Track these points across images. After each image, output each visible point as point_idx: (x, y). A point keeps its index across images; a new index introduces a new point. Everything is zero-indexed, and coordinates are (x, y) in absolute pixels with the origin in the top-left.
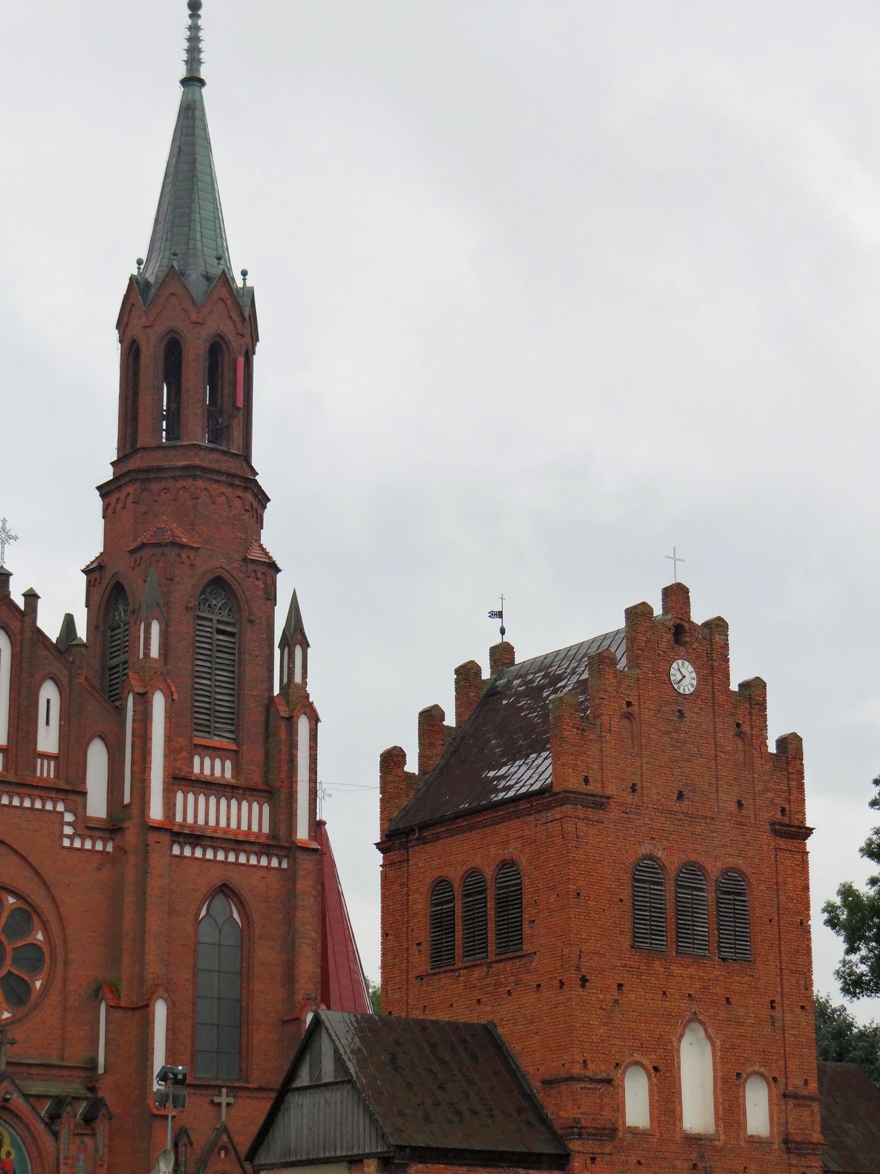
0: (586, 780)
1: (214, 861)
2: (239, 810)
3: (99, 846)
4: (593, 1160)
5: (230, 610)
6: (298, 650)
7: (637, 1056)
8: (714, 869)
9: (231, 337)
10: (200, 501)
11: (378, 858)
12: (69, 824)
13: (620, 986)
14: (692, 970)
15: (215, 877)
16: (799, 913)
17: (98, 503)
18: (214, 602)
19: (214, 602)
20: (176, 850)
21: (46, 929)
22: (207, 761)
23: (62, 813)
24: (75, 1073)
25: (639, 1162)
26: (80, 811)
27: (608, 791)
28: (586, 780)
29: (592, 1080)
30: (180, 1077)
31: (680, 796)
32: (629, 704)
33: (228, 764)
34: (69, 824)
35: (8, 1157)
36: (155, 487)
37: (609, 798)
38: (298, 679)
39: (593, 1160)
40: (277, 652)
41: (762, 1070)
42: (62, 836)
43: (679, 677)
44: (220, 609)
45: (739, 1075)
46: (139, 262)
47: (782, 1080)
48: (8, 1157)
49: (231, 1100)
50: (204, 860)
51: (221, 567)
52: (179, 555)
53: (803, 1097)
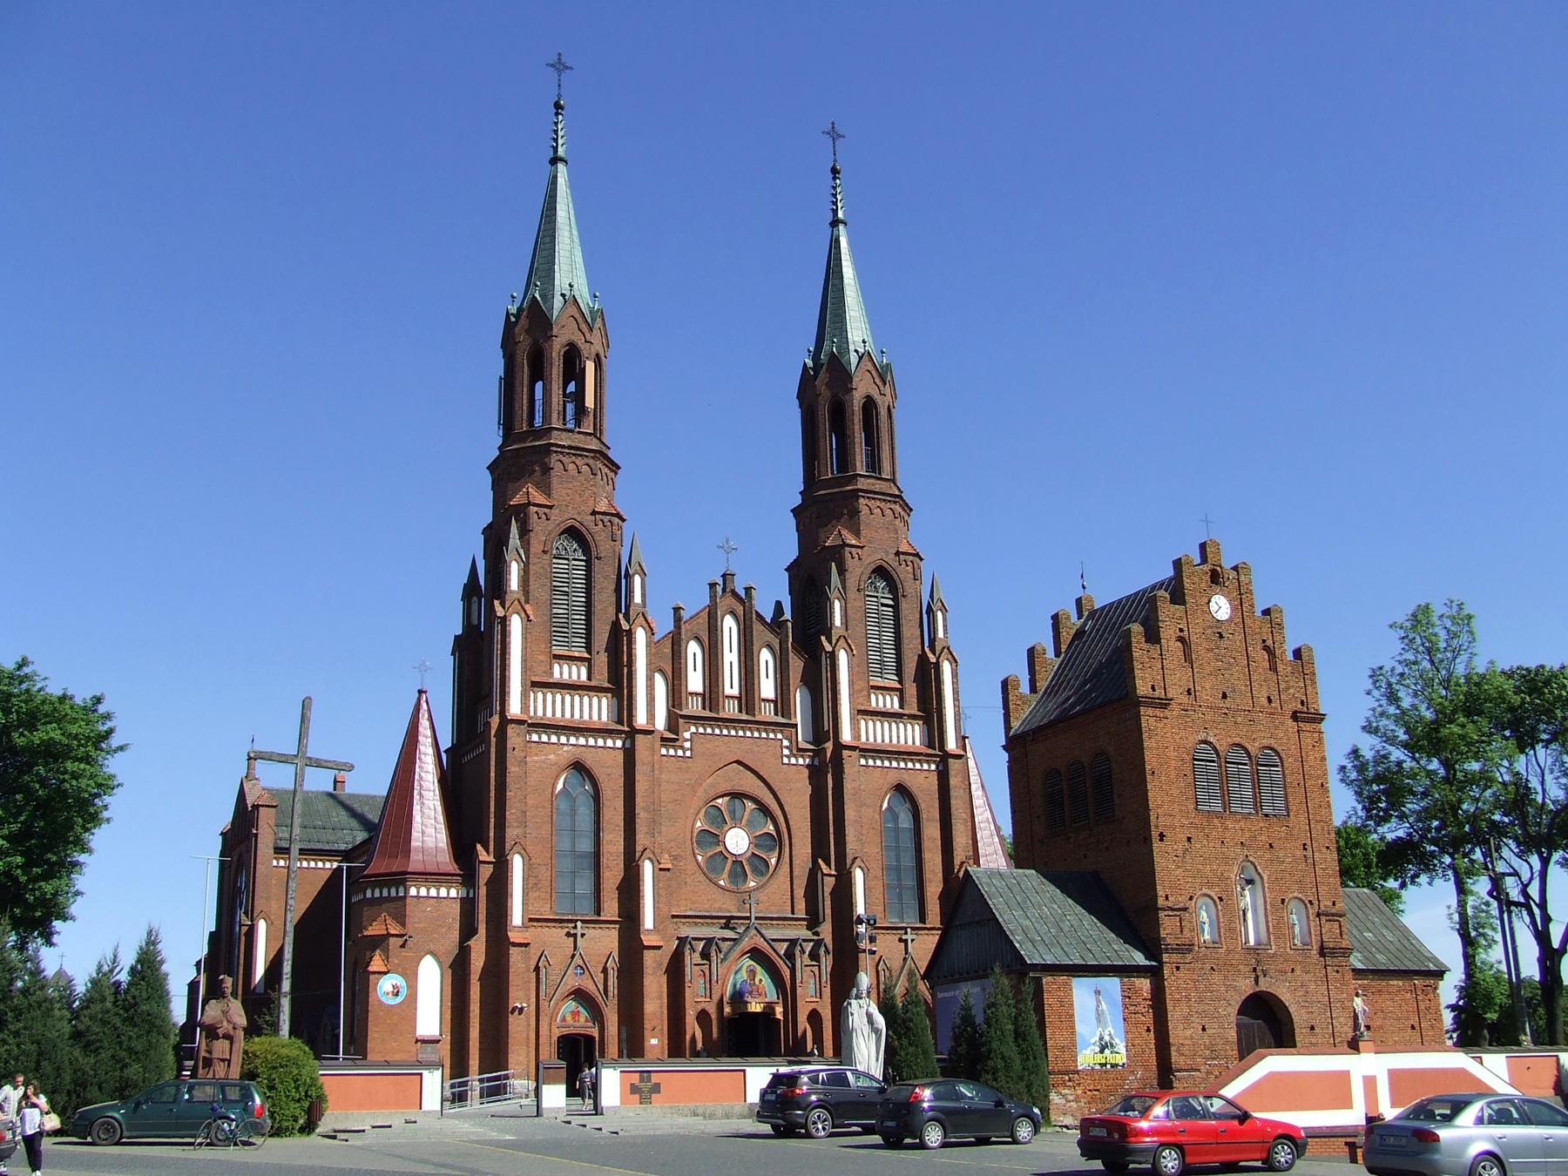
0: (1154, 690)
4: (1178, 968)
7: (1205, 891)
9: (877, 396)
12: (787, 747)
13: (1189, 839)
15: (893, 778)
16: (1319, 777)
17: (792, 522)
18: (878, 584)
19: (878, 584)
20: (863, 762)
25: (1212, 968)
27: (1170, 695)
28: (1153, 688)
31: (1224, 696)
34: (787, 747)
35: (760, 983)
37: (1171, 700)
39: (1178, 968)
41: (1300, 895)
43: (1216, 608)
45: (1283, 901)
48: (760, 983)
49: (914, 937)
53: (1333, 915)
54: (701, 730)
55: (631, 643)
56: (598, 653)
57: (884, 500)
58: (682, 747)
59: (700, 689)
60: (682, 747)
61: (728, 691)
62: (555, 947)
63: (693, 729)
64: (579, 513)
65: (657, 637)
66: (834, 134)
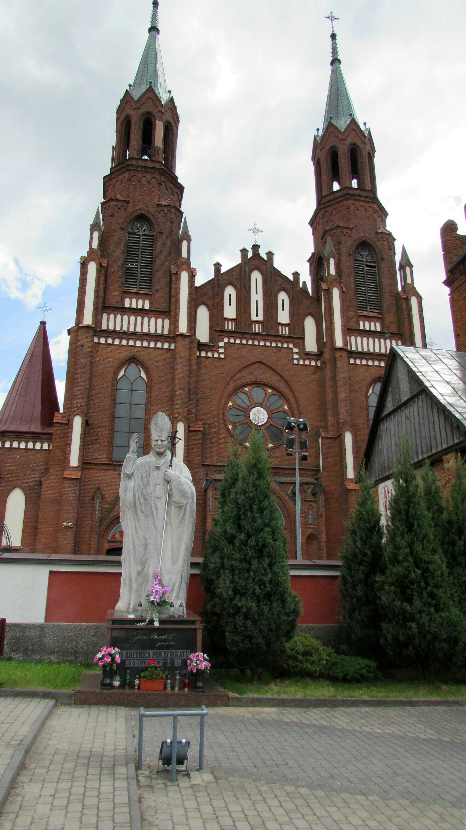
1: (373, 366)
2: (385, 343)
3: (313, 363)
5: (372, 256)
6: (408, 269)
10: (351, 209)
11: (447, 290)
12: (296, 353)
18: (364, 253)
19: (364, 253)
20: (352, 361)
21: (289, 404)
22: (367, 324)
23: (292, 348)
24: (309, 472)
26: (301, 347)
30: (301, 426)
33: (378, 324)
34: (296, 353)
36: (330, 209)
38: (409, 281)
40: (398, 273)
42: (293, 359)
44: (367, 256)
46: (318, 130)
50: (367, 365)
51: (365, 237)
52: (342, 232)
54: (232, 341)
55: (178, 280)
56: (157, 290)
57: (366, 201)
58: (218, 352)
59: (234, 316)
60: (218, 352)
61: (254, 318)
62: (108, 485)
63: (226, 340)
64: (147, 207)
65: (199, 281)
66: (332, 18)
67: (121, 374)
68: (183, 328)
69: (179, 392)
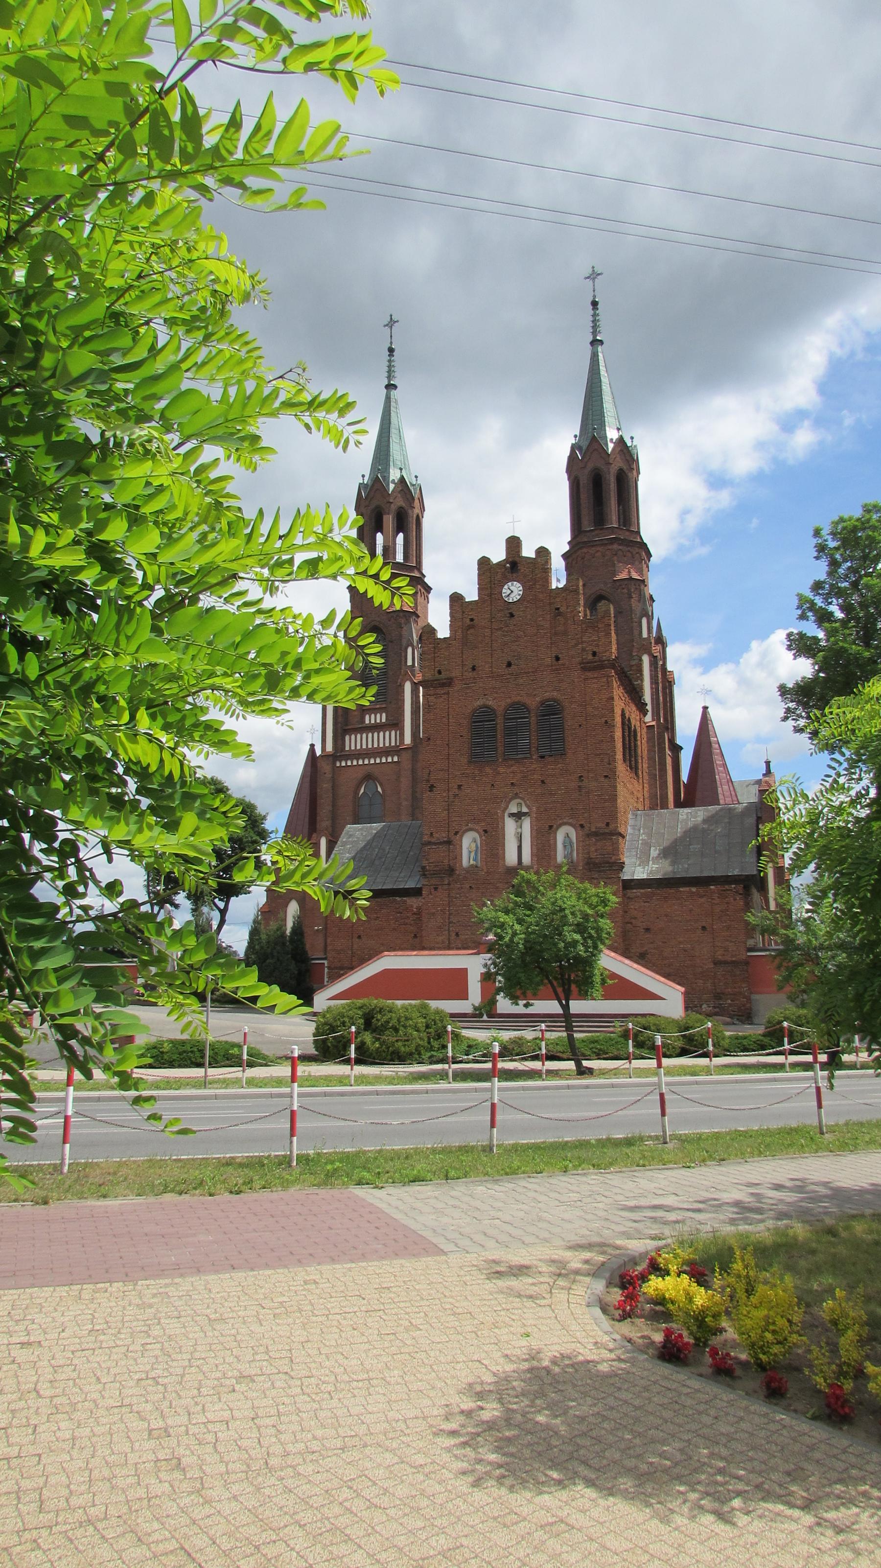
4: (436, 889)
8: (533, 703)
14: (514, 768)
27: (453, 675)
28: (440, 672)
29: (435, 844)
31: (509, 665)
32: (472, 620)
39: (436, 889)
47: (587, 826)
67: (362, 791)
68: (408, 740)
69: (405, 803)
